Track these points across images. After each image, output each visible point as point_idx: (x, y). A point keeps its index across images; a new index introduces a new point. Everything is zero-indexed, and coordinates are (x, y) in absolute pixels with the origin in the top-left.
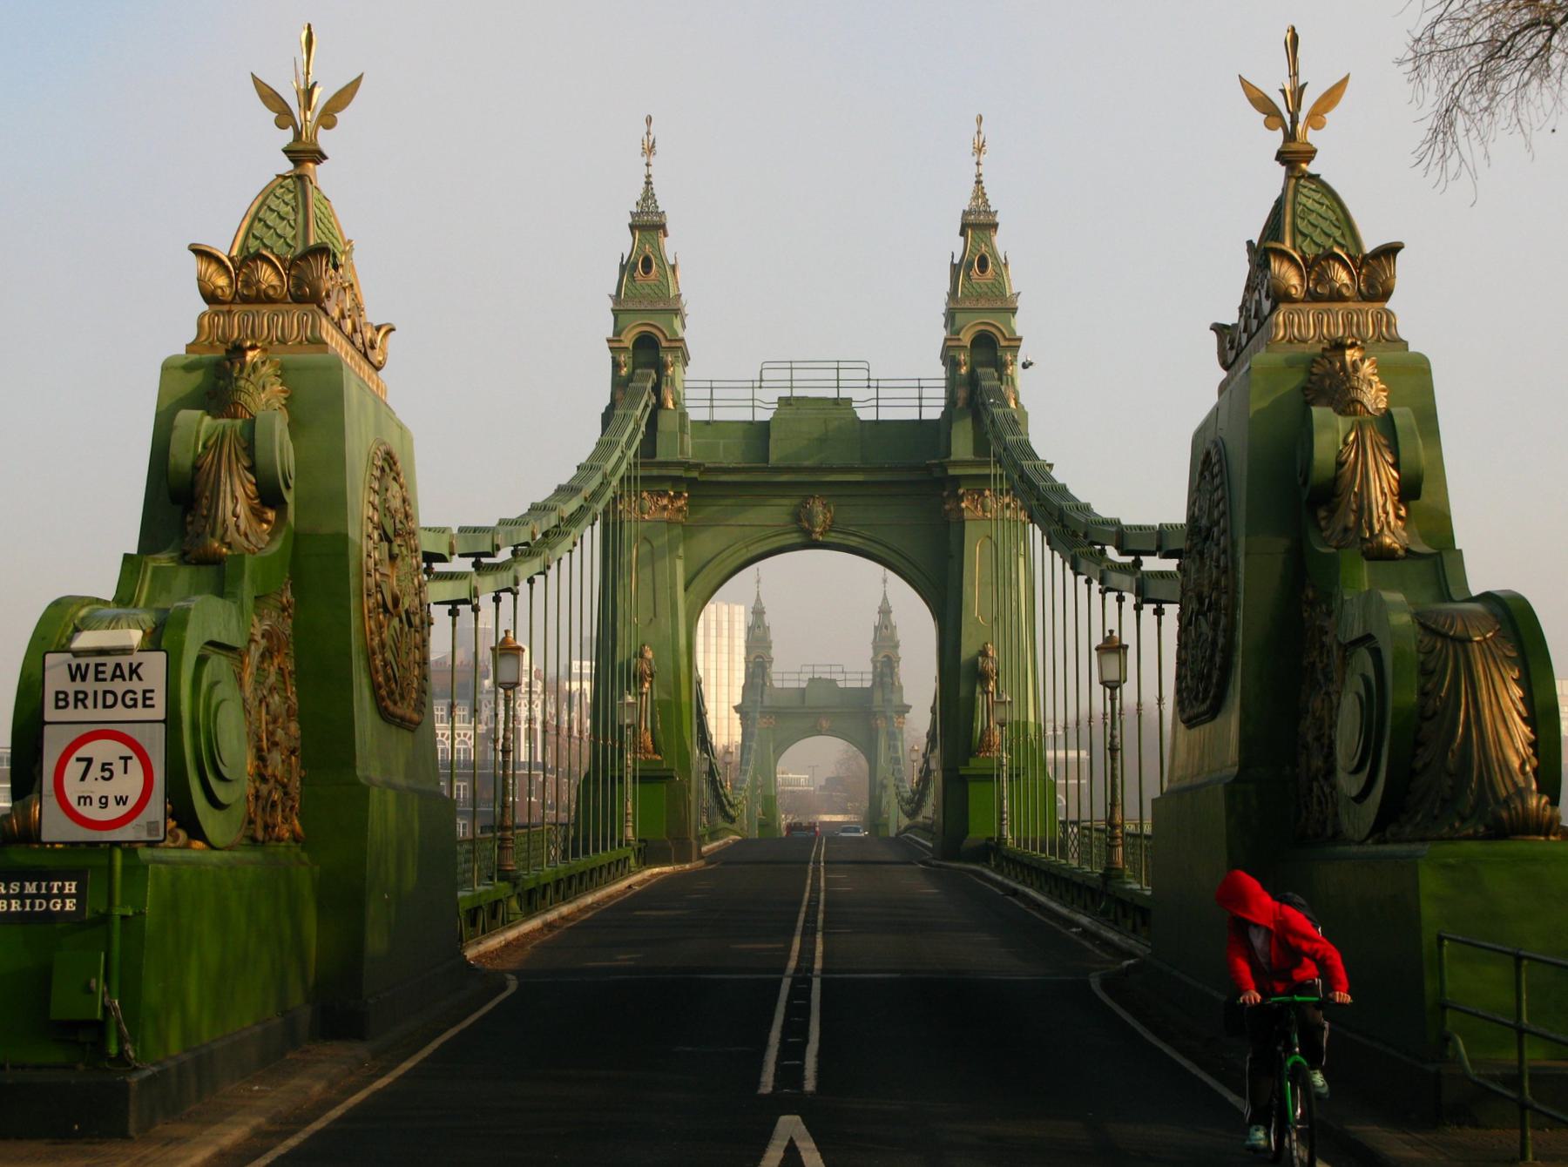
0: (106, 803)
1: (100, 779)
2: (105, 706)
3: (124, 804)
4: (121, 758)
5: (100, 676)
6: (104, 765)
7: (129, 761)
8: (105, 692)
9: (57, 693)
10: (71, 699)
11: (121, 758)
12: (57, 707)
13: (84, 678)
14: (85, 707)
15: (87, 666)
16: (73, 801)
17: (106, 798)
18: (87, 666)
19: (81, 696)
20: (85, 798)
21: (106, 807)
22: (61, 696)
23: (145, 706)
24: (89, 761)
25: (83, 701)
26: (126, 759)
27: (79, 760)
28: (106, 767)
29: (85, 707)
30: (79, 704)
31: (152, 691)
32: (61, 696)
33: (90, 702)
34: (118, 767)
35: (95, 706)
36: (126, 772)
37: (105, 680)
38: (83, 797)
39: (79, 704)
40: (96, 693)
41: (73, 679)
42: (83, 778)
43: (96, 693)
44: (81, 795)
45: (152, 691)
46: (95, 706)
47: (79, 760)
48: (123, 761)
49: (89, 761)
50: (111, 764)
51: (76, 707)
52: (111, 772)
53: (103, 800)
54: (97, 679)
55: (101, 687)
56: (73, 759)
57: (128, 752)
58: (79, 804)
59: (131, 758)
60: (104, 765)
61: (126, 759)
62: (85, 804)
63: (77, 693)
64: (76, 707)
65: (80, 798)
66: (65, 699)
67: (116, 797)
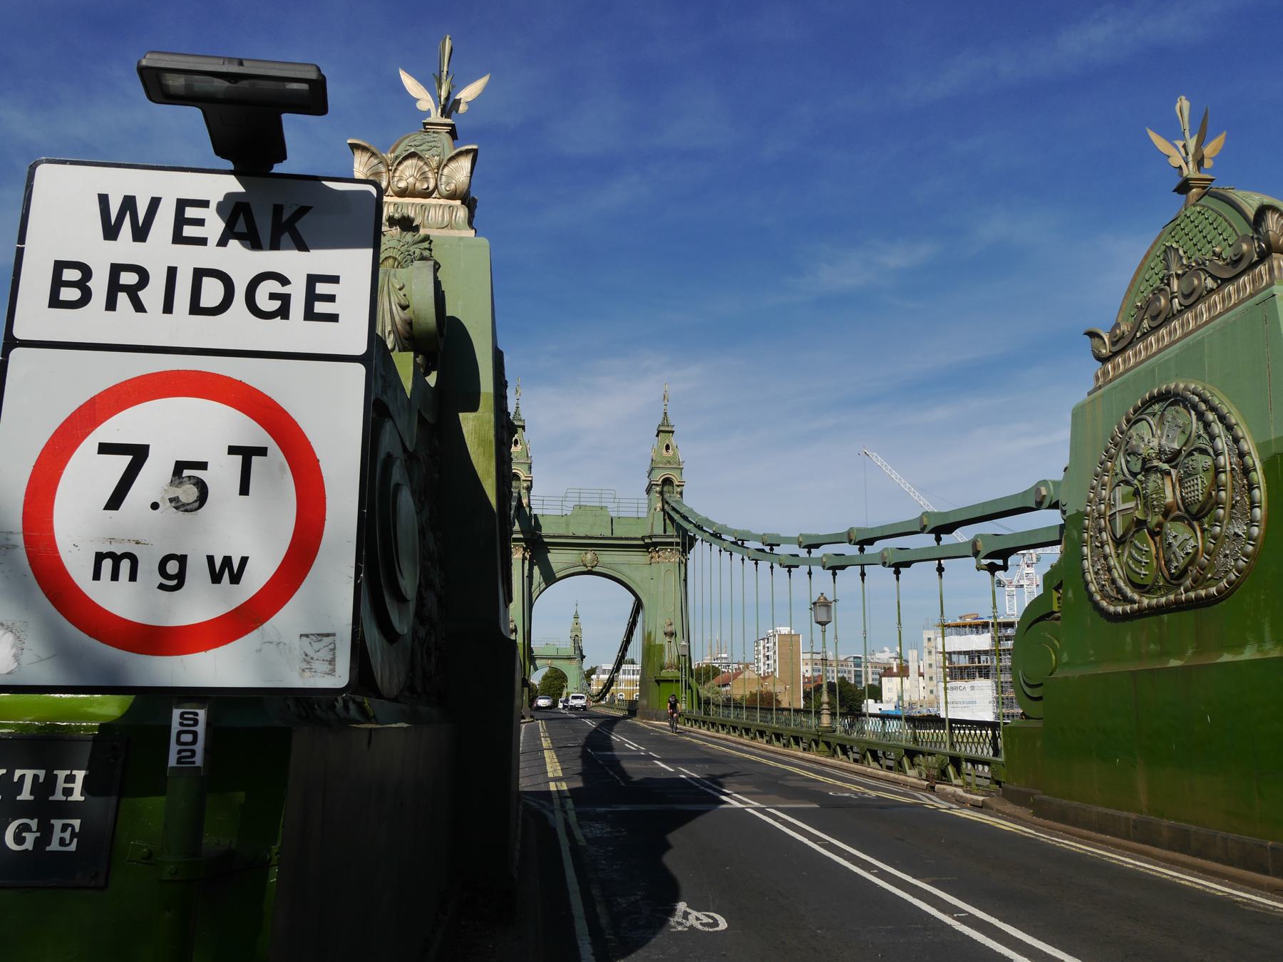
0: (181, 578)
1: (165, 506)
2: (196, 309)
3: (235, 579)
4: (233, 450)
5: (188, 231)
6: (180, 467)
7: (255, 460)
8: (199, 274)
9: (60, 266)
10: (99, 285)
11: (233, 450)
12: (55, 302)
13: (140, 234)
14: (139, 307)
15: (155, 203)
16: (78, 566)
17: (182, 560)
18: (155, 203)
19: (128, 278)
20: (117, 559)
21: (179, 586)
22: (71, 275)
23: (310, 315)
24: (139, 454)
25: (133, 292)
26: (247, 454)
27: (105, 449)
28: (186, 473)
29: (139, 307)
30: (123, 298)
31: (334, 279)
32: (71, 275)
33: (153, 295)
34: (223, 473)
35: (168, 308)
36: (244, 490)
37: (202, 241)
38: (111, 555)
39: (123, 298)
40: (172, 273)
41: (111, 232)
42: (115, 502)
43: (172, 273)
44: (105, 549)
45: (334, 279)
46: (168, 308)
47: (105, 449)
48: (239, 458)
49: (139, 454)
50: (203, 466)
51: (111, 305)
52: (202, 488)
53: (172, 567)
54: (178, 238)
55: (188, 259)
56: (89, 445)
57: (252, 433)
58: (97, 576)
59: (262, 451)
60: (180, 467)
61: (247, 454)
62: (115, 577)
63: (116, 270)
64: (111, 305)
65: (100, 557)
66: (82, 285)
67: (211, 559)
